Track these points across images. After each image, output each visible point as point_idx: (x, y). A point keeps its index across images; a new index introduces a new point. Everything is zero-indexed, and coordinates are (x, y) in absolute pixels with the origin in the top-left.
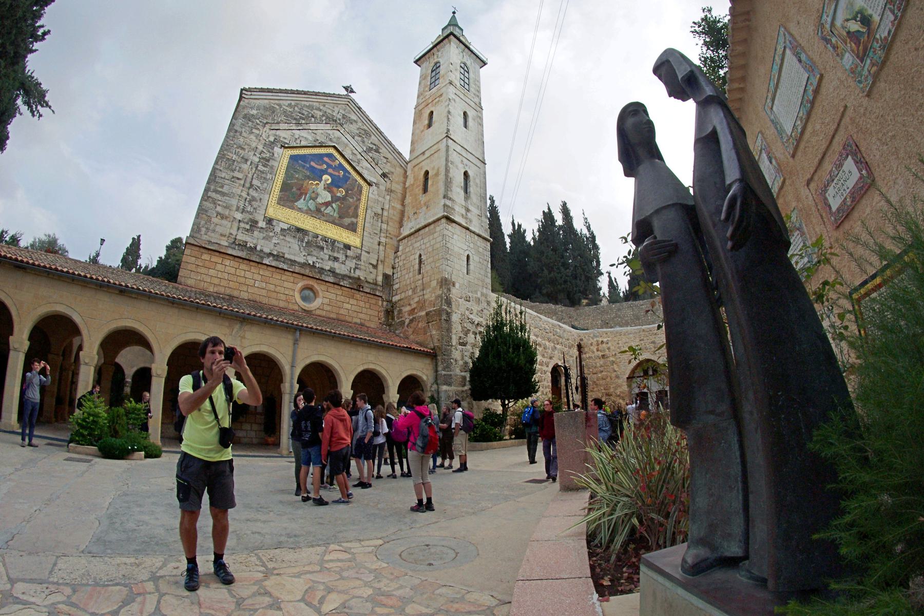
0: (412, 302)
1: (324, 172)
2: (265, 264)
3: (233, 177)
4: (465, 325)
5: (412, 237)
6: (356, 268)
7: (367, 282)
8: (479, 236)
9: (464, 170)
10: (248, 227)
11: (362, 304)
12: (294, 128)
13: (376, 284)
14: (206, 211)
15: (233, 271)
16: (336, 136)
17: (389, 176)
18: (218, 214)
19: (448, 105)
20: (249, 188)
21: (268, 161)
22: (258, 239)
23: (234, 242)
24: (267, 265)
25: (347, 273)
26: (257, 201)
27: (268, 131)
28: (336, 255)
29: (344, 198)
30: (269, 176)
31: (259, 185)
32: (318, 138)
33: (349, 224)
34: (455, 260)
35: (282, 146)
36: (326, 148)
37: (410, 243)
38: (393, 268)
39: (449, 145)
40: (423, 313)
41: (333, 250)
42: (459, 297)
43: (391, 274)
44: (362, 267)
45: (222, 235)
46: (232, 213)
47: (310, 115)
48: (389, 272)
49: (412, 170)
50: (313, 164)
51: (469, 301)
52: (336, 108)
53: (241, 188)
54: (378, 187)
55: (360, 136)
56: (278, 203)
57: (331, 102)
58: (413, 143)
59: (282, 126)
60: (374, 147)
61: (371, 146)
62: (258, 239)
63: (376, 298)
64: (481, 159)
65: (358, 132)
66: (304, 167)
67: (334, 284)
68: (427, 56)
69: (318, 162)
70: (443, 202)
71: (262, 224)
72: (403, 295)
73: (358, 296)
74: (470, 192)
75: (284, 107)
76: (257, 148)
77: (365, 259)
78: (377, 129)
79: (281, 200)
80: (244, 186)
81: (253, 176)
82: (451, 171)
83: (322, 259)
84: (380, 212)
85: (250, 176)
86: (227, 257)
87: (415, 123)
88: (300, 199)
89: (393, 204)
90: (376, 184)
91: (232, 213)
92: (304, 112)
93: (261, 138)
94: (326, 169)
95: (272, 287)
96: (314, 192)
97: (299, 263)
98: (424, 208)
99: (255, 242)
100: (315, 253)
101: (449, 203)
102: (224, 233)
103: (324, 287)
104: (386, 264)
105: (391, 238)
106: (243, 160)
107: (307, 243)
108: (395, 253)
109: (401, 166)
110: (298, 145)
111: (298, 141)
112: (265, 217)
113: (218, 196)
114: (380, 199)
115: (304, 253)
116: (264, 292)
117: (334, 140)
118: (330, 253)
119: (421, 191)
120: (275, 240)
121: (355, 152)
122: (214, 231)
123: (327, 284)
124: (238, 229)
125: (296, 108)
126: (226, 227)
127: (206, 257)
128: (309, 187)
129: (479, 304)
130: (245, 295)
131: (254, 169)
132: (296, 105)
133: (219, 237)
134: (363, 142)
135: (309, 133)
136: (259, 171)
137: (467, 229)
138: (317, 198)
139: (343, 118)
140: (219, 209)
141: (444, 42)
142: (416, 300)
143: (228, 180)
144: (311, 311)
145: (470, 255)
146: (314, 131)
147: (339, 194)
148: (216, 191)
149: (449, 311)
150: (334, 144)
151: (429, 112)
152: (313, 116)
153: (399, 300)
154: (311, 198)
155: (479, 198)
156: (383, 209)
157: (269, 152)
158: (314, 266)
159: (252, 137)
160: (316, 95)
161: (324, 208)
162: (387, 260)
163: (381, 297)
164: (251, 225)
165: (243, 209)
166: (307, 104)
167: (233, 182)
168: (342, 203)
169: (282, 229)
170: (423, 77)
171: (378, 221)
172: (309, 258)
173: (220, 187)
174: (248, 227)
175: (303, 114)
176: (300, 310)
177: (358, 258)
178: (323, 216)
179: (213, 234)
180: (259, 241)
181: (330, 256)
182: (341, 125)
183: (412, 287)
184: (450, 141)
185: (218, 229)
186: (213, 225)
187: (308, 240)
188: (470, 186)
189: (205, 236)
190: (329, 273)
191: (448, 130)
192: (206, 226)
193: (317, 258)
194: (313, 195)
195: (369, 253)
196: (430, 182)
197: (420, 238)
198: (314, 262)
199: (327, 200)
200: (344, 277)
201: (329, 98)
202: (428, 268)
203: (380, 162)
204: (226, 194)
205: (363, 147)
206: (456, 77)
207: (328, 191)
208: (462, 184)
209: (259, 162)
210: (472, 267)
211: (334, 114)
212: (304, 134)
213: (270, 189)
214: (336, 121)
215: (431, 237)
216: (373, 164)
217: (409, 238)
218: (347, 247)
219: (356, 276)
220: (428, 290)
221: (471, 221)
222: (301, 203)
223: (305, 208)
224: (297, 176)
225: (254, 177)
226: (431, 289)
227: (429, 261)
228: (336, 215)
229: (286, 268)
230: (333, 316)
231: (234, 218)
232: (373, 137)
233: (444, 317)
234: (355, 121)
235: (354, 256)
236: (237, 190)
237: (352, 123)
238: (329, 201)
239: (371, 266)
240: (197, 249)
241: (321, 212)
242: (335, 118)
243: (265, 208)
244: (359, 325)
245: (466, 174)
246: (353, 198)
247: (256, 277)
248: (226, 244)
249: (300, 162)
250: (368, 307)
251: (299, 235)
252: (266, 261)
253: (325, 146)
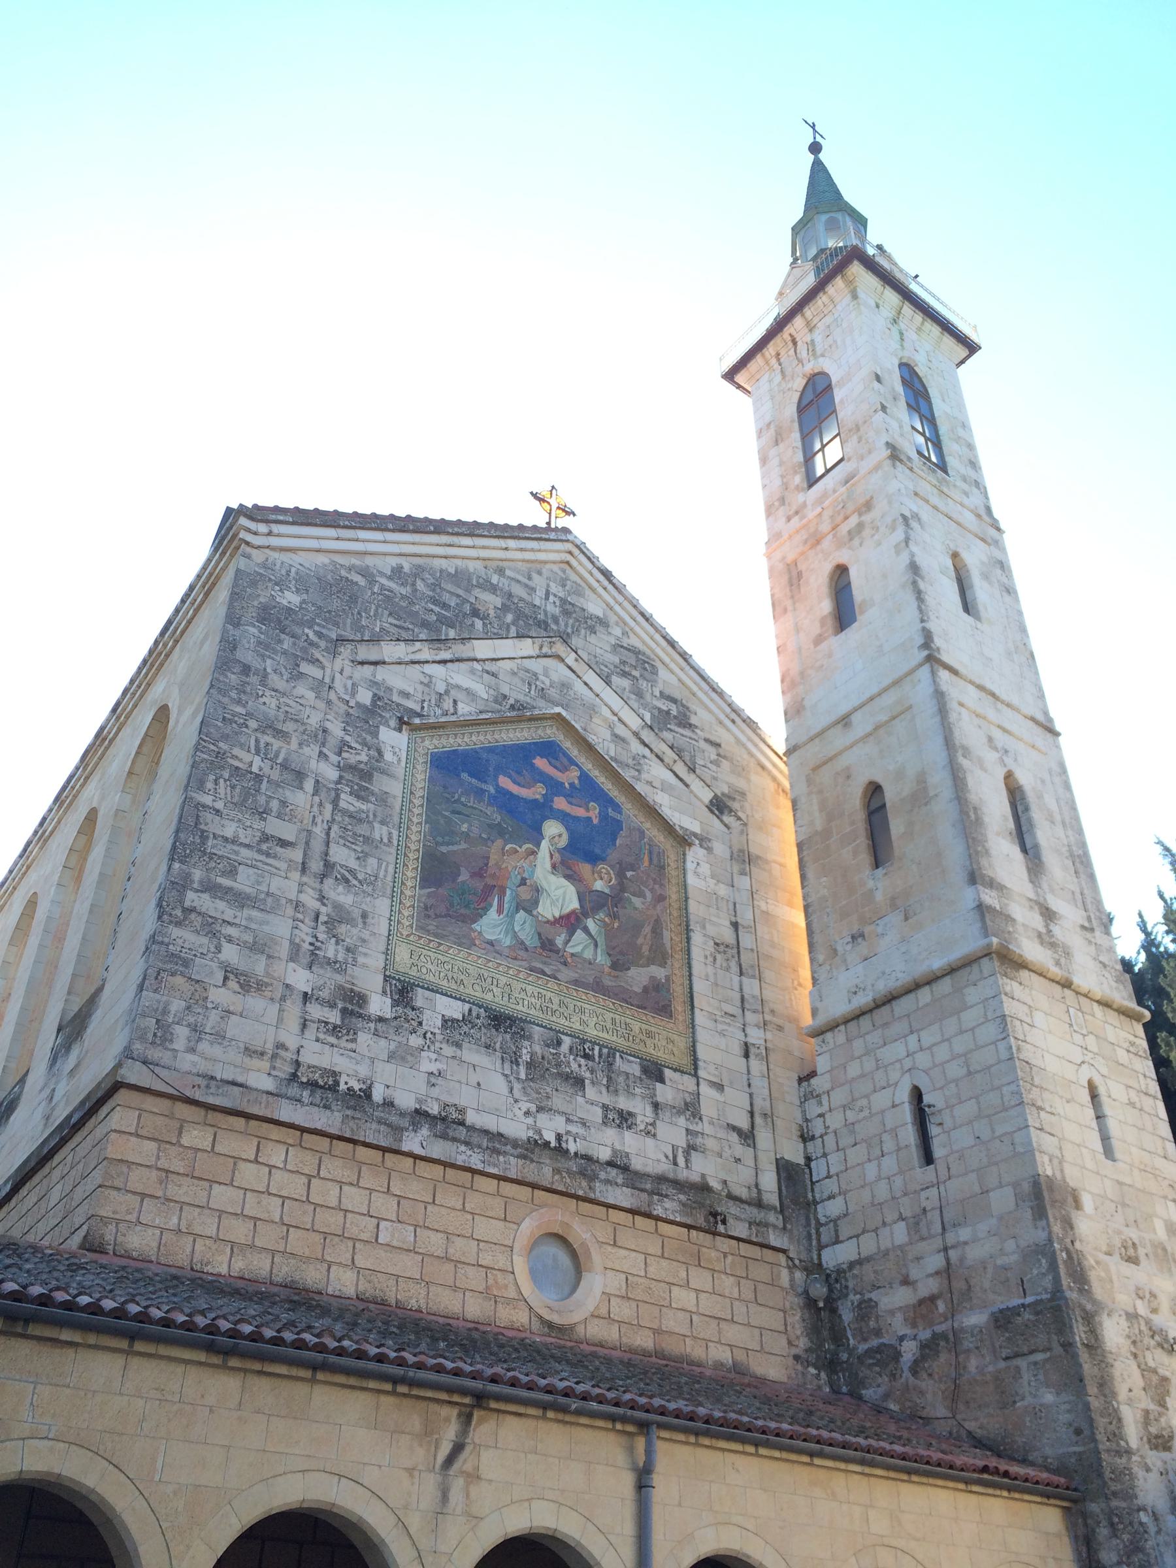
0: (915, 1273)
1: (542, 810)
2: (410, 1155)
3: (266, 838)
4: (1151, 1364)
5: (865, 1022)
6: (691, 1148)
7: (731, 1197)
8: (1105, 1004)
9: (1004, 771)
10: (334, 1017)
11: (728, 1283)
12: (426, 655)
13: (759, 1204)
14: (186, 963)
15: (296, 1187)
16: (555, 677)
17: (730, 803)
18: (229, 972)
19: (907, 540)
20: (323, 877)
21: (367, 775)
22: (372, 1060)
23: (294, 1077)
24: (416, 1157)
25: (664, 1168)
26: (350, 921)
27: (348, 670)
28: (623, 1103)
30: (380, 832)
31: (353, 864)
32: (505, 690)
33: (646, 990)
34: (1060, 1106)
35: (401, 722)
36: (533, 724)
37: (858, 1046)
38: (806, 1138)
39: (944, 688)
40: (975, 1319)
41: (611, 1087)
42: (1104, 1248)
43: (802, 1161)
44: (711, 1144)
45: (249, 1051)
46: (278, 969)
47: (467, 608)
48: (794, 1153)
49: (809, 781)
50: (505, 782)
51: (1133, 1260)
52: (535, 576)
53: (296, 875)
54: (709, 850)
55: (625, 674)
56: (419, 928)
57: (519, 555)
58: (789, 683)
59: (392, 651)
61: (663, 705)
62: (372, 1060)
63: (769, 1255)
64: (1040, 717)
65: (617, 660)
66: (480, 793)
67: (633, 1212)
68: (770, 350)
69: (519, 773)
70: (969, 896)
71: (379, 1005)
72: (868, 1245)
73: (713, 1254)
74: (1036, 846)
75: (384, 581)
76: (325, 731)
77: (713, 1113)
78: (672, 644)
79: (429, 917)
80: (304, 869)
81: (328, 834)
82: (971, 782)
83: (584, 1124)
84: (728, 935)
85: (319, 830)
86: (275, 1132)
87: (779, 609)
88: (486, 910)
89: (764, 907)
90: (704, 841)
91: (278, 969)
92: (446, 597)
93: (332, 696)
94: (548, 799)
95: (434, 1242)
96: (523, 882)
97: (515, 1144)
98: (895, 918)
99: (363, 1071)
100: (558, 1101)
101: (989, 898)
102: (257, 1044)
103: (603, 1232)
104: (778, 1122)
105: (780, 1028)
106: (288, 777)
107: (530, 1065)
108: (800, 1080)
109: (763, 767)
110: (453, 718)
111: (448, 704)
112: (386, 978)
113: (221, 905)
115: (525, 1106)
116: (408, 1265)
117: (553, 693)
118: (606, 1099)
119: (865, 858)
120: (428, 1064)
121: (621, 730)
122: (220, 1036)
123: (615, 1215)
124: (304, 1026)
125: (420, 585)
127: (196, 1137)
128: (510, 863)
129: (1170, 1270)
130: (344, 1283)
131: (329, 807)
132: (418, 572)
133: (239, 1059)
134: (639, 694)
135: (473, 671)
136: (345, 812)
137: (1067, 984)
138: (536, 903)
139: (566, 613)
140: (230, 953)
141: (830, 289)
142: (936, 1262)
143: (247, 846)
144: (571, 1328)
145: (1098, 1081)
146: (489, 666)
147: (599, 885)
148: (209, 888)
149: (1089, 1307)
150: (558, 710)
151: (828, 567)
152: (475, 613)
153: (852, 1265)
154: (519, 906)
155: (1069, 863)
156: (735, 925)
157: (364, 744)
158: (560, 1151)
159: (303, 690)
160: (471, 535)
161: (563, 935)
162: (780, 1109)
163: (784, 1251)
164: (344, 1011)
165: (313, 953)
166: (450, 566)
167: (268, 855)
168: (615, 916)
169: (445, 1021)
170: (772, 435)
171: (728, 969)
172: (543, 1120)
173: (224, 874)
174: (334, 1017)
175: (445, 606)
176: (536, 1325)
177: (691, 1108)
178: (565, 964)
179: (217, 1051)
180: (379, 1066)
181: (605, 1108)
182: (565, 639)
183: (907, 1213)
184: (944, 675)
185: (235, 1028)
186: (214, 1016)
187: (532, 1054)
188: (1031, 825)
189: (190, 1057)
190: (613, 1172)
191: (928, 636)
192: (192, 1020)
193: (568, 1120)
194: (525, 894)
195: (720, 1087)
196: (897, 827)
197: (900, 1027)
198: (559, 1137)
199: (566, 911)
200: (662, 1184)
201: (511, 543)
202: (963, 1138)
203: (700, 761)
204: (248, 897)
205: (641, 711)
206: (901, 427)
207: (568, 877)
208: (1011, 825)
209: (338, 782)
210: (1113, 1125)
211: (537, 602)
212: (460, 676)
213: (389, 878)
214: (546, 623)
215: (951, 1025)
216: (681, 769)
217: (852, 1026)
218: (654, 1072)
219: (695, 1177)
220: (983, 1228)
221: (1068, 954)
222: (490, 925)
223: (508, 943)
224: (465, 827)
225: (332, 834)
226: (994, 1221)
227: (966, 1110)
228: (601, 959)
229: (480, 1167)
230: (644, 1340)
231: (287, 986)
232: (663, 673)
233: (1079, 1333)
234: (603, 622)
235: (679, 1103)
236: (287, 885)
237: (593, 631)
238: (573, 912)
239: (734, 1137)
240: (163, 1105)
241: (557, 952)
242: (541, 617)
243: (382, 948)
244: (729, 1371)
245: (1009, 777)
246: (641, 895)
247: (385, 1206)
248: (268, 1084)
249: (464, 776)
250: (751, 1296)
251: (501, 1038)
252: (413, 1142)
253: (532, 719)
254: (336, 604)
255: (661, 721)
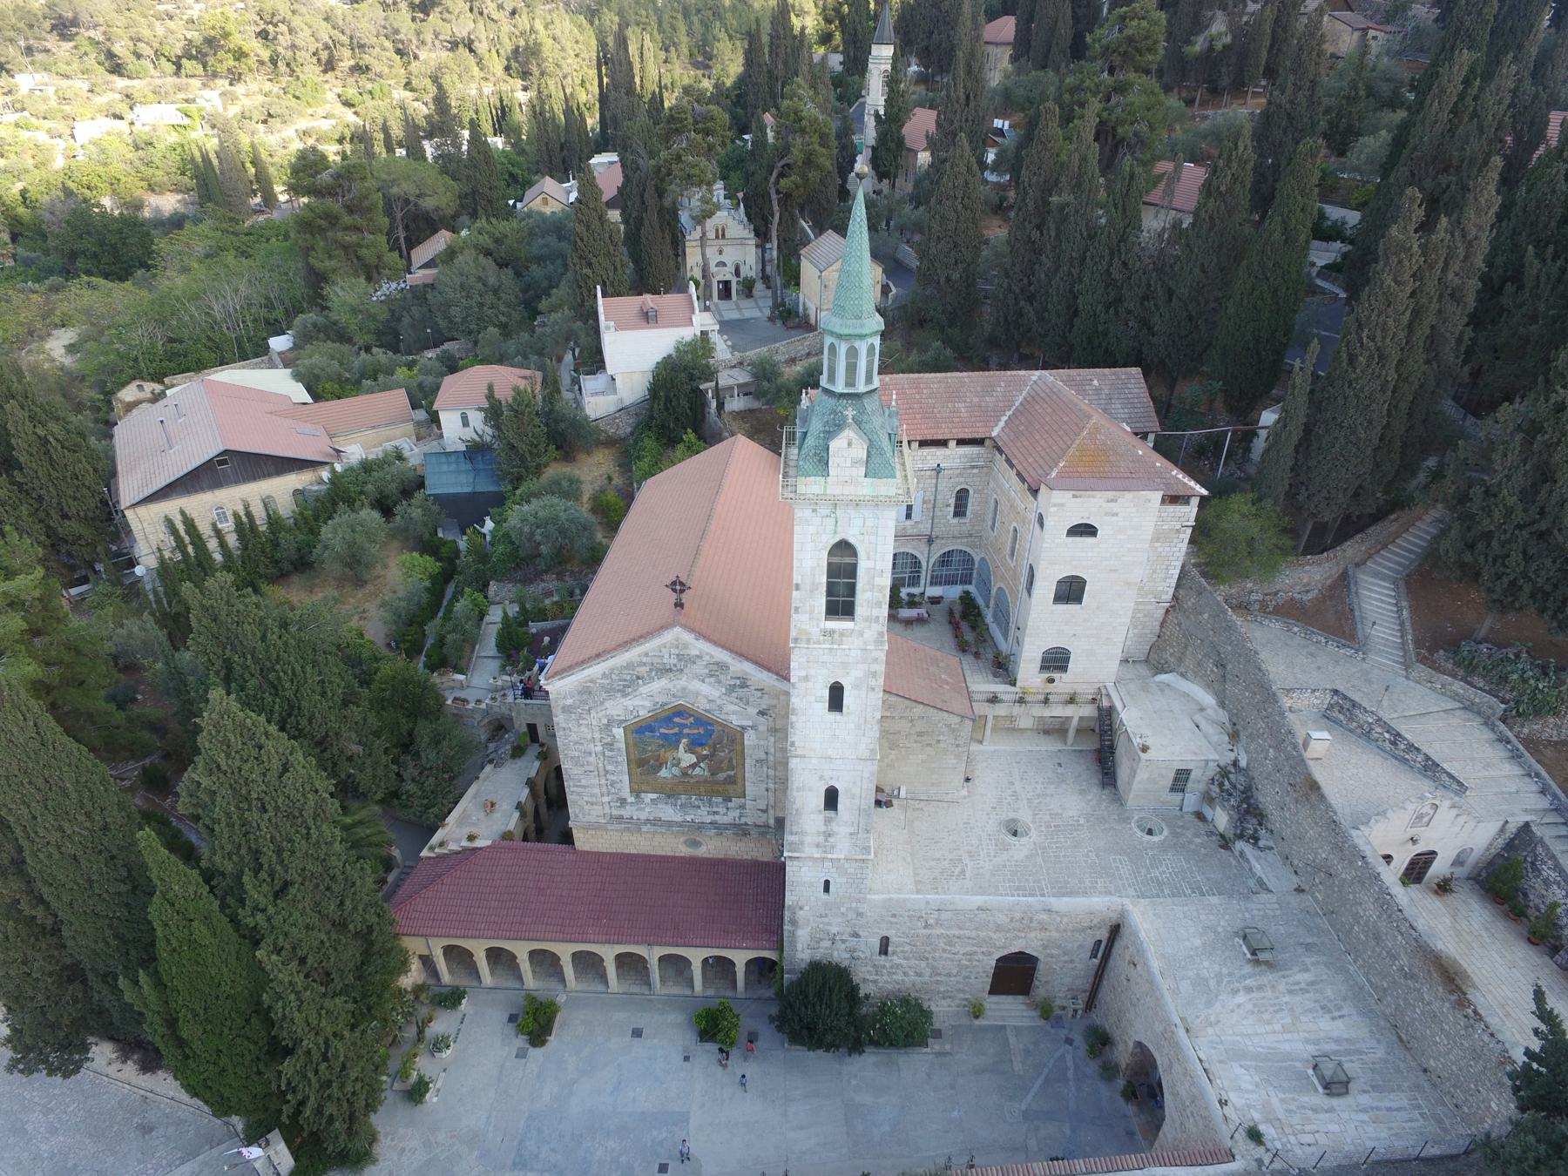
1: (679, 736)
29: (711, 757)
30: (620, 759)
55: (711, 676)
60: (738, 682)
90: (752, 727)
114: (762, 742)
117: (679, 694)
120: (648, 810)
126: (598, 810)
139: (680, 660)
152: (638, 678)
237: (694, 663)
254: (585, 697)
255: (732, 688)
